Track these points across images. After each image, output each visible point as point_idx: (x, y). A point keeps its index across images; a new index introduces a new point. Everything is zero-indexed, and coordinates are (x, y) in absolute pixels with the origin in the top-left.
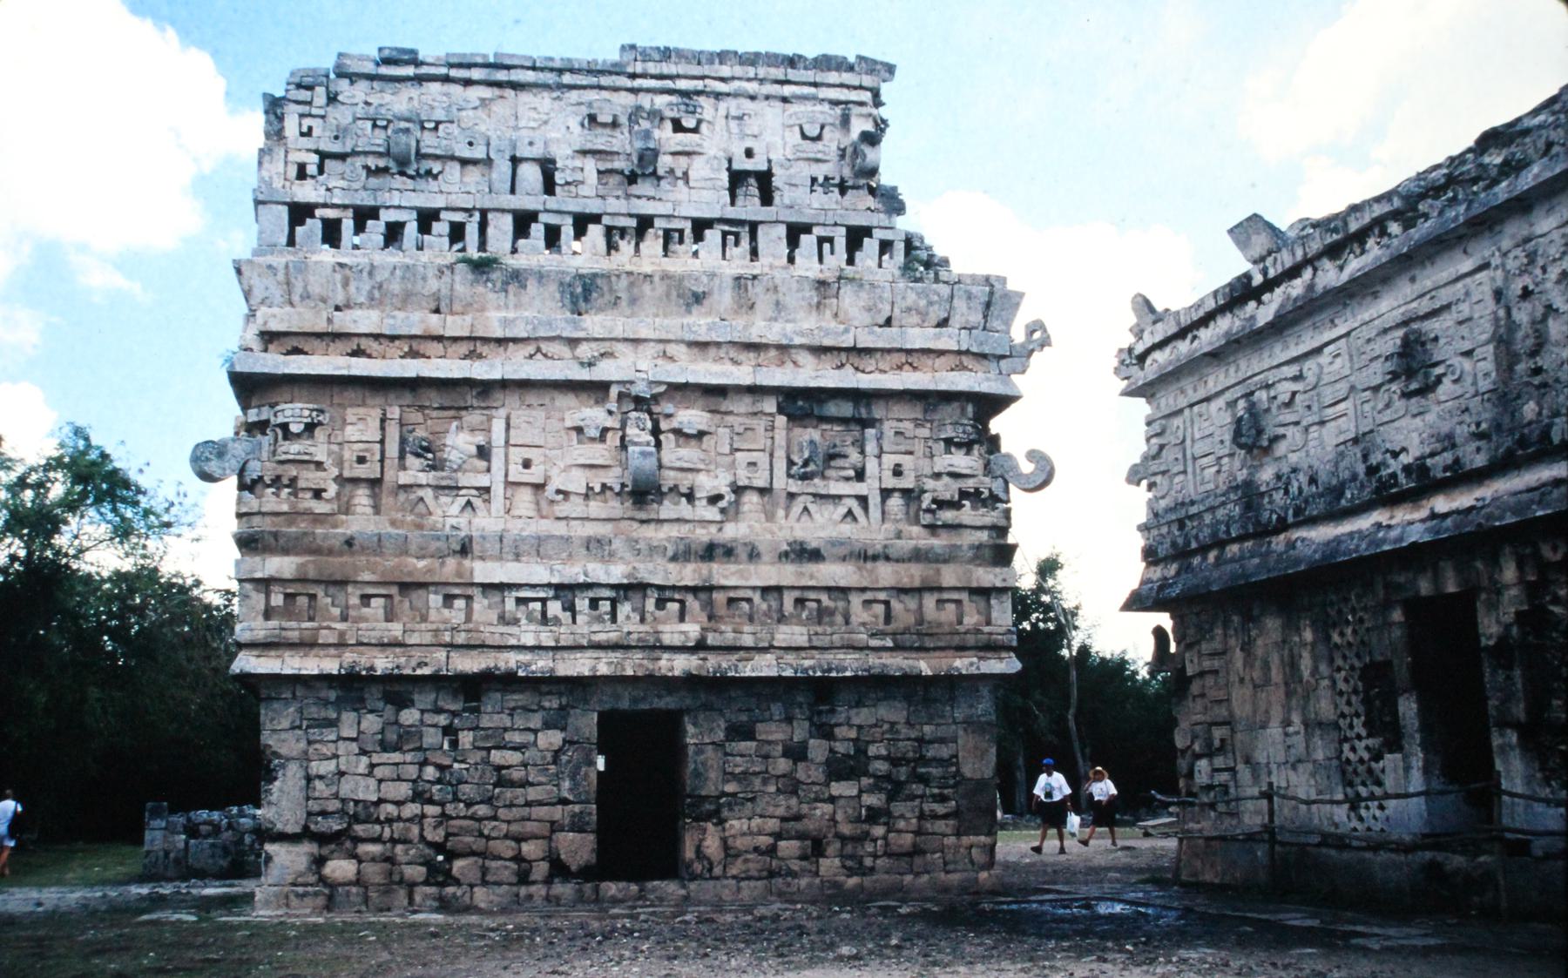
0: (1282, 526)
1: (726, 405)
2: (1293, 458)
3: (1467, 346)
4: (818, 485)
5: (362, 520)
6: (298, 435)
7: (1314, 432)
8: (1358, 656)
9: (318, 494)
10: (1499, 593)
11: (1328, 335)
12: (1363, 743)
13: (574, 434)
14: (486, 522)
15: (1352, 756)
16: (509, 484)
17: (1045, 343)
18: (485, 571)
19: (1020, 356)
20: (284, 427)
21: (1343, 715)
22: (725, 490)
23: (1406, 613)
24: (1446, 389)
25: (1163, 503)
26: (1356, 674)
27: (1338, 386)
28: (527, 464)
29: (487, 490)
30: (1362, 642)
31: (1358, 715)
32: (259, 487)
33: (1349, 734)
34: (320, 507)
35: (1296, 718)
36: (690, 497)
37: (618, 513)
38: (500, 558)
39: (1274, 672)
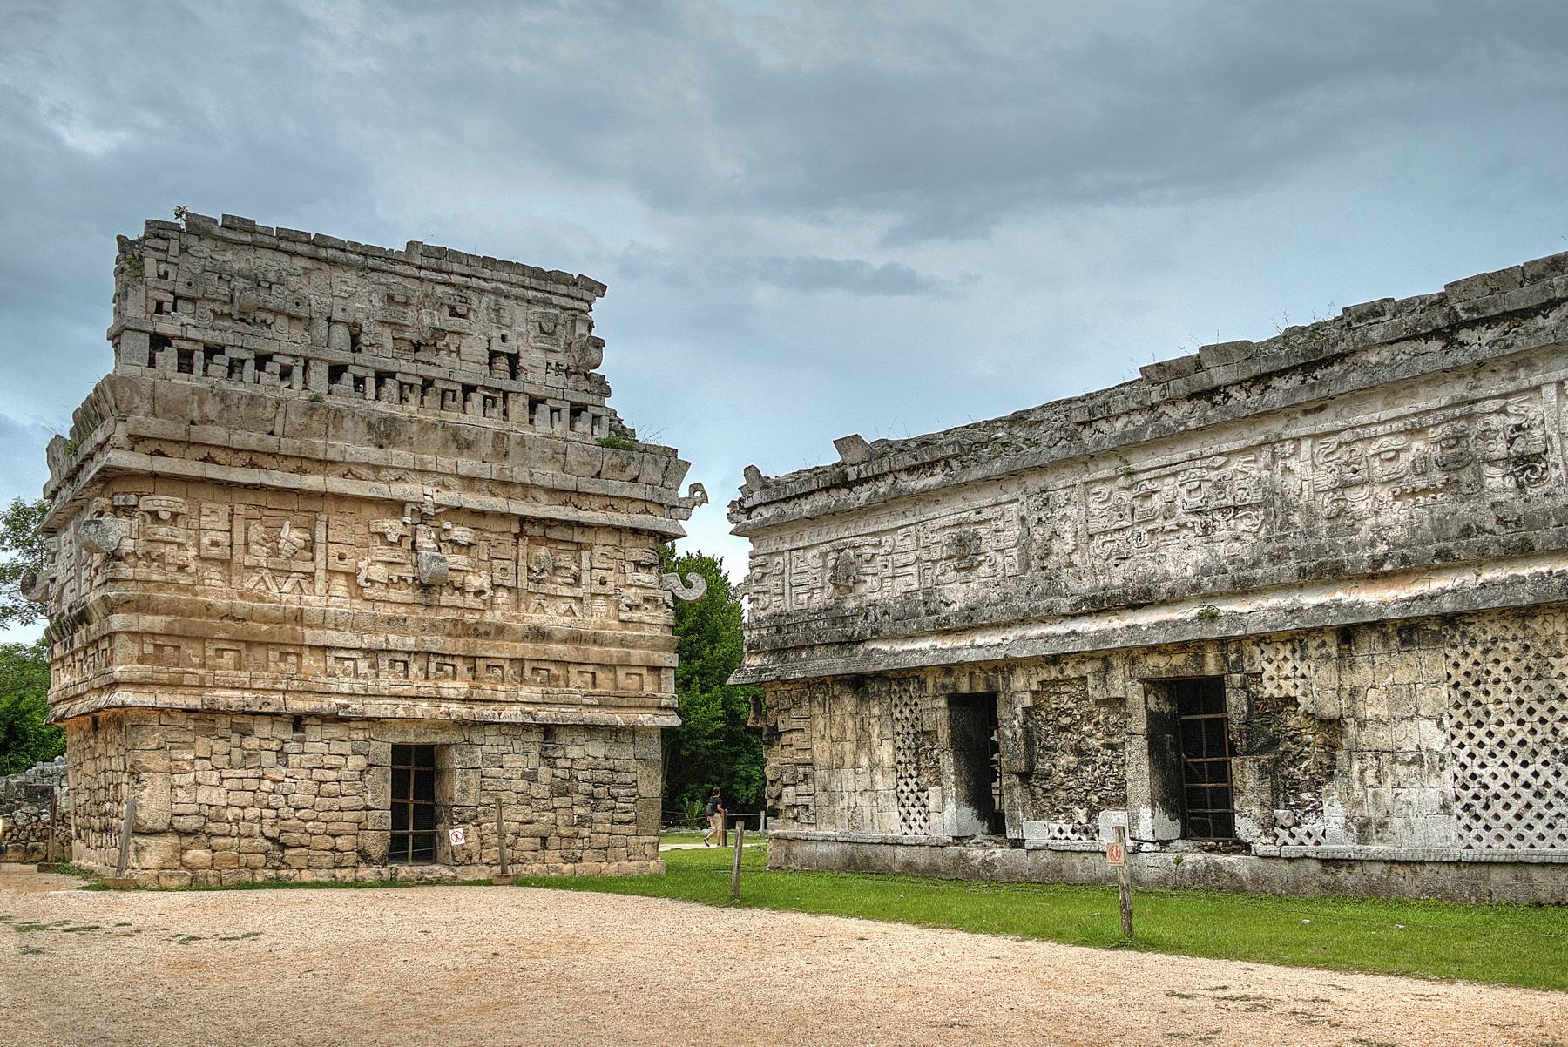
0: (861, 640)
1: (484, 524)
2: (872, 597)
4: (548, 588)
5: (216, 589)
6: (164, 522)
7: (888, 582)
9: (182, 568)
13: (377, 538)
14: (314, 601)
16: (328, 571)
17: (704, 500)
18: (310, 636)
19: (683, 509)
20: (154, 515)
22: (487, 587)
23: (949, 704)
24: (984, 570)
25: (763, 613)
28: (341, 557)
29: (312, 575)
32: (132, 560)
34: (183, 579)
36: (462, 590)
37: (410, 599)
38: (322, 626)
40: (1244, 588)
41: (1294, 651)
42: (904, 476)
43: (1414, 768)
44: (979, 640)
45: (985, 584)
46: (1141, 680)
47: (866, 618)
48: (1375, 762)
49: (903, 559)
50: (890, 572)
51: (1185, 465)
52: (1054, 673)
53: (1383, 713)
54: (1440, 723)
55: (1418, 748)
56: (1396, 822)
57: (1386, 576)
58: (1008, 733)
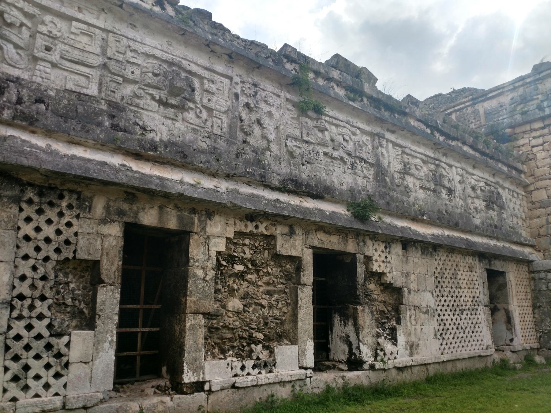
3: (212, 105)
8: (58, 251)
21: (21, 297)
26: (50, 265)
31: (43, 298)
33: (25, 313)
41: (386, 248)
43: (426, 315)
45: (194, 129)
48: (414, 312)
51: (341, 124)
52: (250, 227)
54: (433, 294)
55: (427, 306)
58: (200, 273)
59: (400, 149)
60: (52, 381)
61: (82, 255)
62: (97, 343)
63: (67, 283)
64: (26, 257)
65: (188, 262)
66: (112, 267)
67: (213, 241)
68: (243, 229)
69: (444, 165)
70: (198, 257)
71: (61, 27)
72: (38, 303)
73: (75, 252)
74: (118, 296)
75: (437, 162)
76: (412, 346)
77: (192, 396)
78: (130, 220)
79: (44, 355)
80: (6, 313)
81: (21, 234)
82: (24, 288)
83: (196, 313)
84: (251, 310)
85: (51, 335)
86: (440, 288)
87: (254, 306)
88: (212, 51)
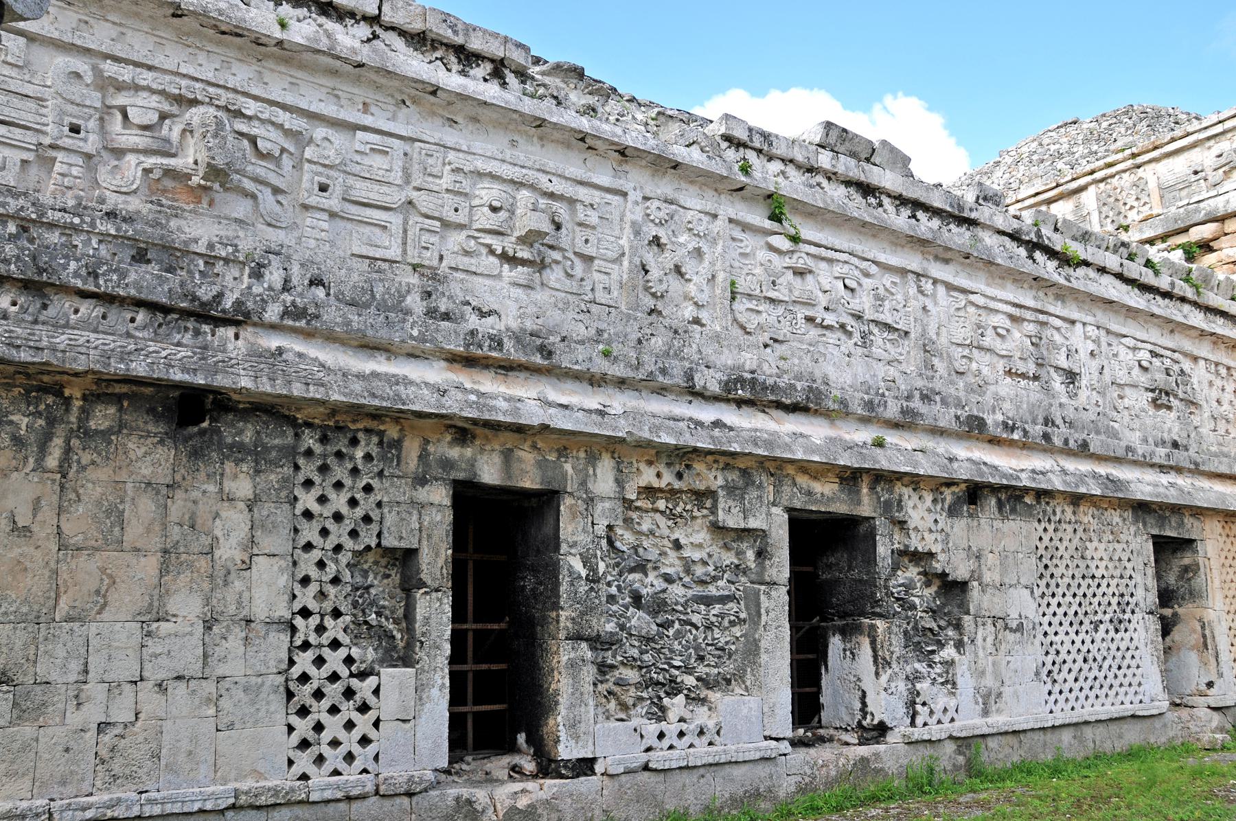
0: (239, 319)
3: (590, 250)
8: (354, 534)
10: (590, 501)
11: (368, 120)
12: (342, 653)
15: (312, 671)
21: (305, 613)
26: (345, 558)
27: (385, 189)
30: (367, 519)
33: (313, 639)
35: (187, 606)
39: (134, 532)
40: (906, 422)
41: (935, 501)
42: (398, 43)
43: (1018, 635)
44: (553, 395)
46: (789, 510)
47: (257, 274)
49: (362, 191)
50: (332, 201)
53: (997, 579)
54: (1032, 592)
56: (1007, 691)
57: (1012, 443)
59: (961, 296)
60: (357, 749)
61: (389, 541)
62: (420, 688)
63: (367, 588)
64: (309, 547)
65: (557, 548)
66: (435, 560)
67: (599, 507)
68: (656, 484)
69: (1058, 323)
70: (575, 538)
71: (335, 145)
72: (329, 622)
73: (379, 535)
74: (448, 609)
75: (1041, 317)
76: (986, 697)
77: (575, 780)
78: (461, 476)
79: (343, 707)
80: (285, 638)
81: (299, 508)
82: (307, 597)
83: (577, 637)
84: (671, 632)
85: (352, 675)
86: (1047, 579)
87: (677, 625)
88: (589, 148)
